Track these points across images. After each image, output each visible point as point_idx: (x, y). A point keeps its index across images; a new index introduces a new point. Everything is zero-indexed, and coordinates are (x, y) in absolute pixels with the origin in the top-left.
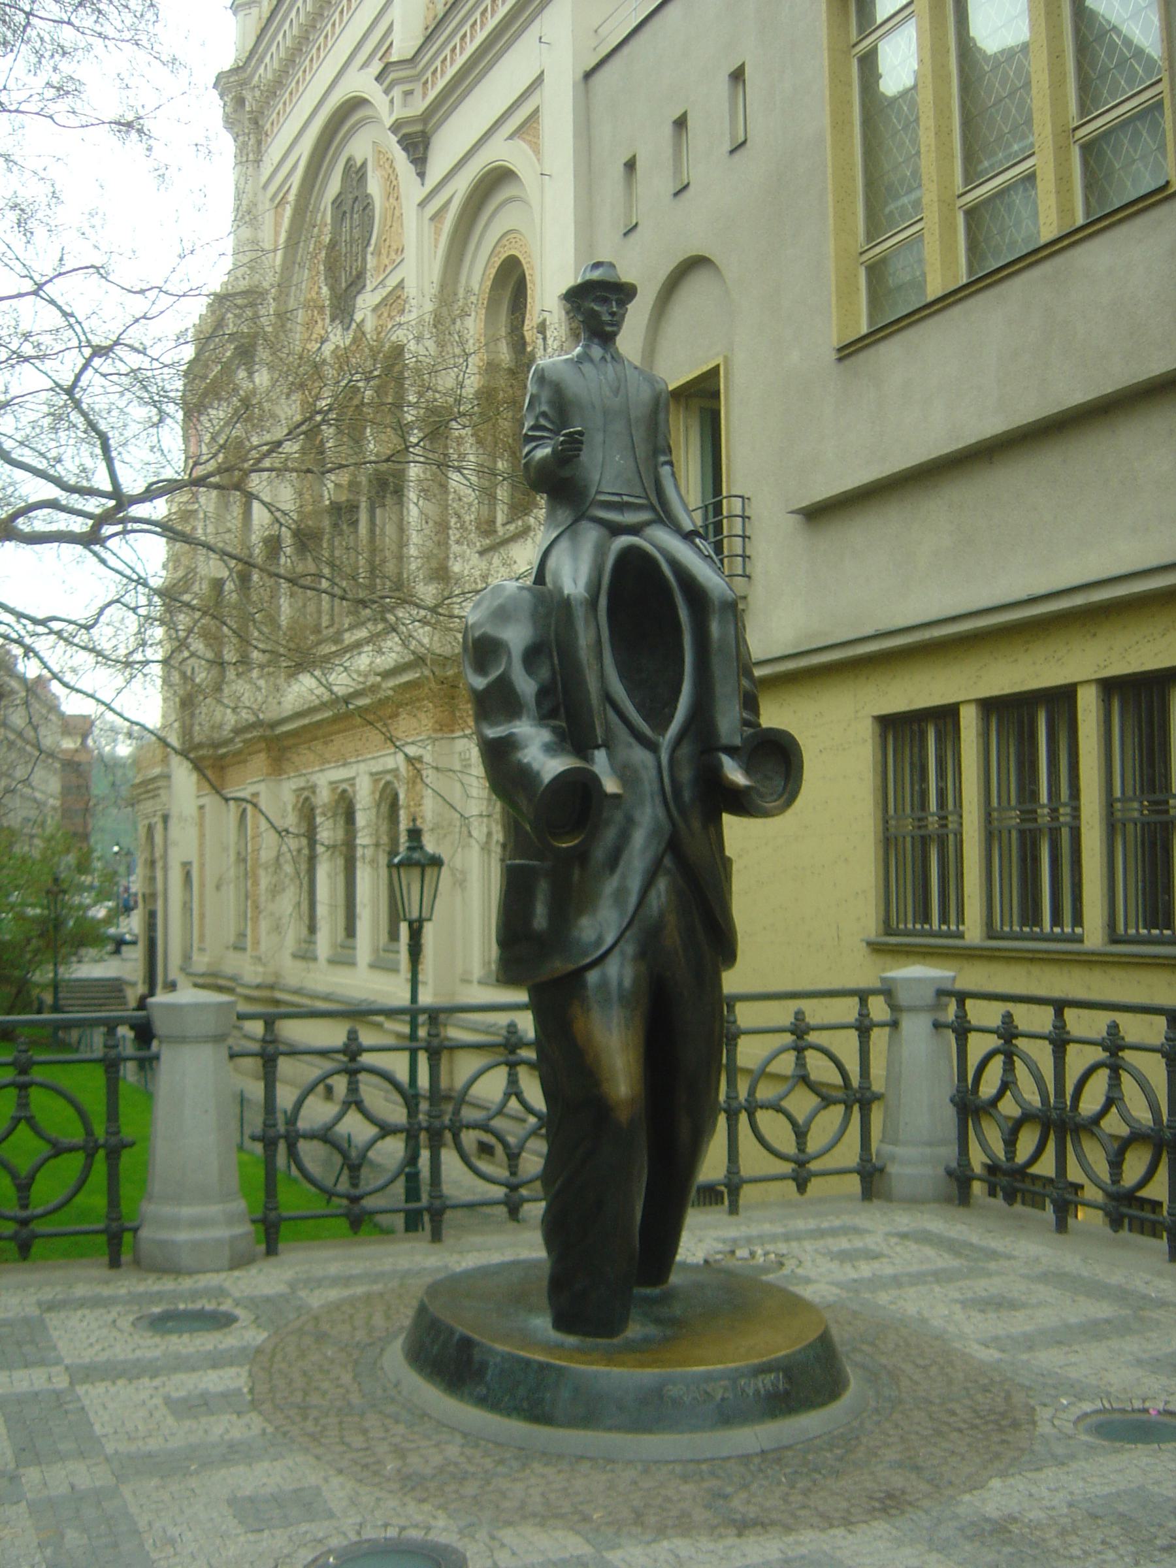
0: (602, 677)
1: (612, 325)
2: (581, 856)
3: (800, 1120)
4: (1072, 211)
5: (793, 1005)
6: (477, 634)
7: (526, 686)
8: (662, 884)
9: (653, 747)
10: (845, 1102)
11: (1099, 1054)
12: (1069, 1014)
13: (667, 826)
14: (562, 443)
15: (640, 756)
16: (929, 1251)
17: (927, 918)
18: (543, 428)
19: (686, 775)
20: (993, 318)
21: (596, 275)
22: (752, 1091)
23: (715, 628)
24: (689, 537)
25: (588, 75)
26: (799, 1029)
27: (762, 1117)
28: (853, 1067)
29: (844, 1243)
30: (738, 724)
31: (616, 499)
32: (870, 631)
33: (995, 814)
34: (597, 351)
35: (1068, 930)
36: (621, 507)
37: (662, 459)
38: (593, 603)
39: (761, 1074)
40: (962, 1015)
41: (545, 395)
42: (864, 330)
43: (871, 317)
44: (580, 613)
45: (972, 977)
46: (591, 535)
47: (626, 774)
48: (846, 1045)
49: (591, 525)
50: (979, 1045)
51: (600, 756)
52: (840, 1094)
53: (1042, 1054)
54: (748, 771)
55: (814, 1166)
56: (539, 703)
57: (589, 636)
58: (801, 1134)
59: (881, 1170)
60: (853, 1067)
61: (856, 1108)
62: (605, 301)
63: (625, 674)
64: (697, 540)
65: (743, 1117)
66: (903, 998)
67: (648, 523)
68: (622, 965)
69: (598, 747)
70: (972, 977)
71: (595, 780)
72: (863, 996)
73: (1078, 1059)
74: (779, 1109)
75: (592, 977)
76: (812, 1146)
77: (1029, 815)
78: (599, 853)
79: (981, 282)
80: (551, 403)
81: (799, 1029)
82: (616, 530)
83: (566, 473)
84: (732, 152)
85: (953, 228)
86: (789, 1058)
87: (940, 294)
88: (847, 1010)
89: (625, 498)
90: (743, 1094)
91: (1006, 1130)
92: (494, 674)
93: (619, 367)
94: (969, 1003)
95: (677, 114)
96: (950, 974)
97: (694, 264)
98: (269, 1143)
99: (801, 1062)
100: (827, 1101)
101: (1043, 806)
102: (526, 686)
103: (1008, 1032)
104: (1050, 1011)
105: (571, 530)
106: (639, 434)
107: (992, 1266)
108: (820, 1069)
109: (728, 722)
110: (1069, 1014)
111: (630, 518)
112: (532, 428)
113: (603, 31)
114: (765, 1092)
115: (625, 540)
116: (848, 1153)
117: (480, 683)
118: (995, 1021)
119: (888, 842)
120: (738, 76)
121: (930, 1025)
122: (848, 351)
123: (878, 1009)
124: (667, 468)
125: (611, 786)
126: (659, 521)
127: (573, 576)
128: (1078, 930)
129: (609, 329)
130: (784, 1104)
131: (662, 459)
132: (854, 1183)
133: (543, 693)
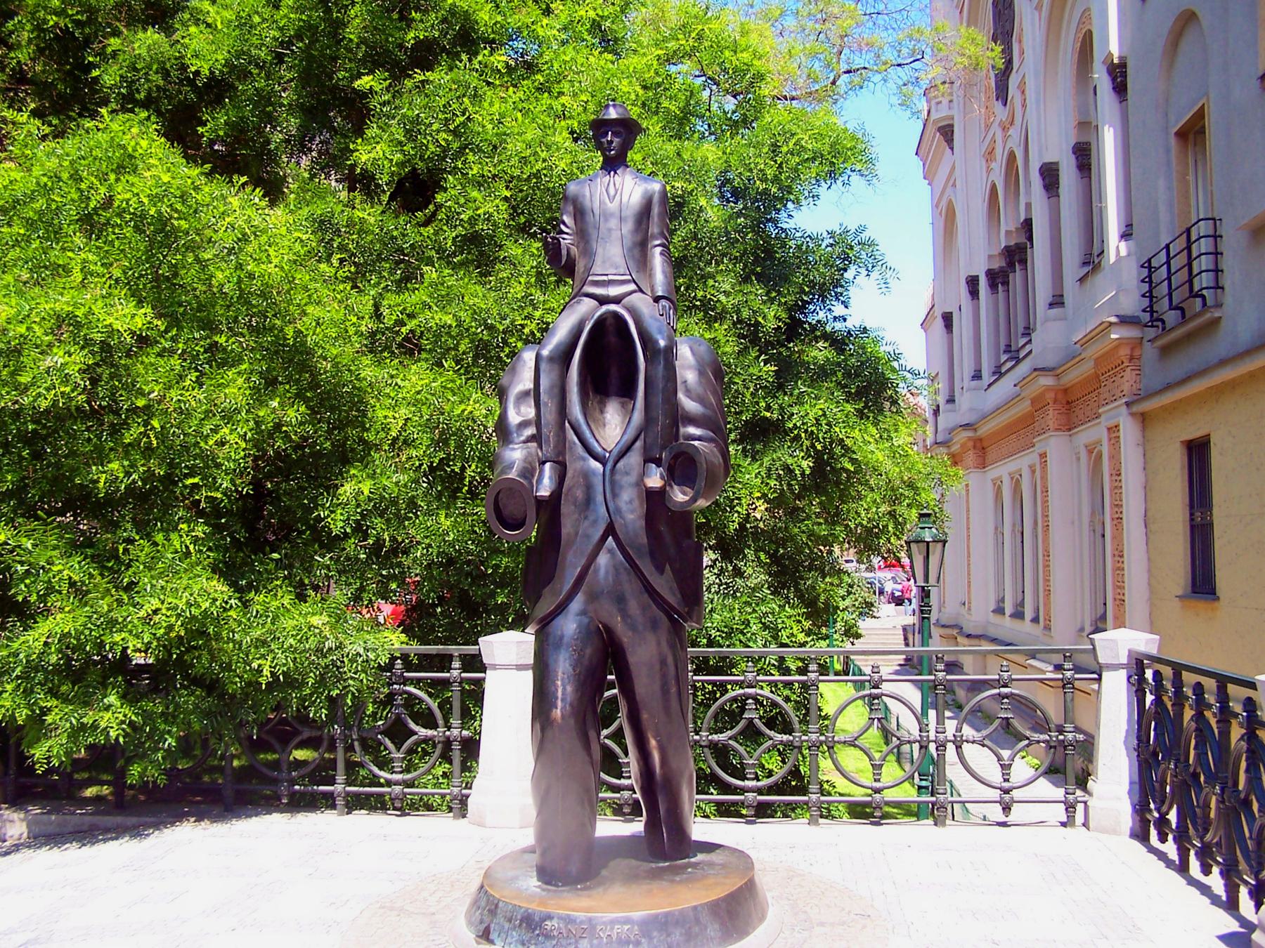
31: (605, 278)
46: (587, 304)
49: (586, 300)
55: (1015, 793)
58: (1006, 768)
65: (951, 748)
89: (611, 277)
106: (628, 227)
111: (613, 291)
115: (605, 308)
126: (641, 291)
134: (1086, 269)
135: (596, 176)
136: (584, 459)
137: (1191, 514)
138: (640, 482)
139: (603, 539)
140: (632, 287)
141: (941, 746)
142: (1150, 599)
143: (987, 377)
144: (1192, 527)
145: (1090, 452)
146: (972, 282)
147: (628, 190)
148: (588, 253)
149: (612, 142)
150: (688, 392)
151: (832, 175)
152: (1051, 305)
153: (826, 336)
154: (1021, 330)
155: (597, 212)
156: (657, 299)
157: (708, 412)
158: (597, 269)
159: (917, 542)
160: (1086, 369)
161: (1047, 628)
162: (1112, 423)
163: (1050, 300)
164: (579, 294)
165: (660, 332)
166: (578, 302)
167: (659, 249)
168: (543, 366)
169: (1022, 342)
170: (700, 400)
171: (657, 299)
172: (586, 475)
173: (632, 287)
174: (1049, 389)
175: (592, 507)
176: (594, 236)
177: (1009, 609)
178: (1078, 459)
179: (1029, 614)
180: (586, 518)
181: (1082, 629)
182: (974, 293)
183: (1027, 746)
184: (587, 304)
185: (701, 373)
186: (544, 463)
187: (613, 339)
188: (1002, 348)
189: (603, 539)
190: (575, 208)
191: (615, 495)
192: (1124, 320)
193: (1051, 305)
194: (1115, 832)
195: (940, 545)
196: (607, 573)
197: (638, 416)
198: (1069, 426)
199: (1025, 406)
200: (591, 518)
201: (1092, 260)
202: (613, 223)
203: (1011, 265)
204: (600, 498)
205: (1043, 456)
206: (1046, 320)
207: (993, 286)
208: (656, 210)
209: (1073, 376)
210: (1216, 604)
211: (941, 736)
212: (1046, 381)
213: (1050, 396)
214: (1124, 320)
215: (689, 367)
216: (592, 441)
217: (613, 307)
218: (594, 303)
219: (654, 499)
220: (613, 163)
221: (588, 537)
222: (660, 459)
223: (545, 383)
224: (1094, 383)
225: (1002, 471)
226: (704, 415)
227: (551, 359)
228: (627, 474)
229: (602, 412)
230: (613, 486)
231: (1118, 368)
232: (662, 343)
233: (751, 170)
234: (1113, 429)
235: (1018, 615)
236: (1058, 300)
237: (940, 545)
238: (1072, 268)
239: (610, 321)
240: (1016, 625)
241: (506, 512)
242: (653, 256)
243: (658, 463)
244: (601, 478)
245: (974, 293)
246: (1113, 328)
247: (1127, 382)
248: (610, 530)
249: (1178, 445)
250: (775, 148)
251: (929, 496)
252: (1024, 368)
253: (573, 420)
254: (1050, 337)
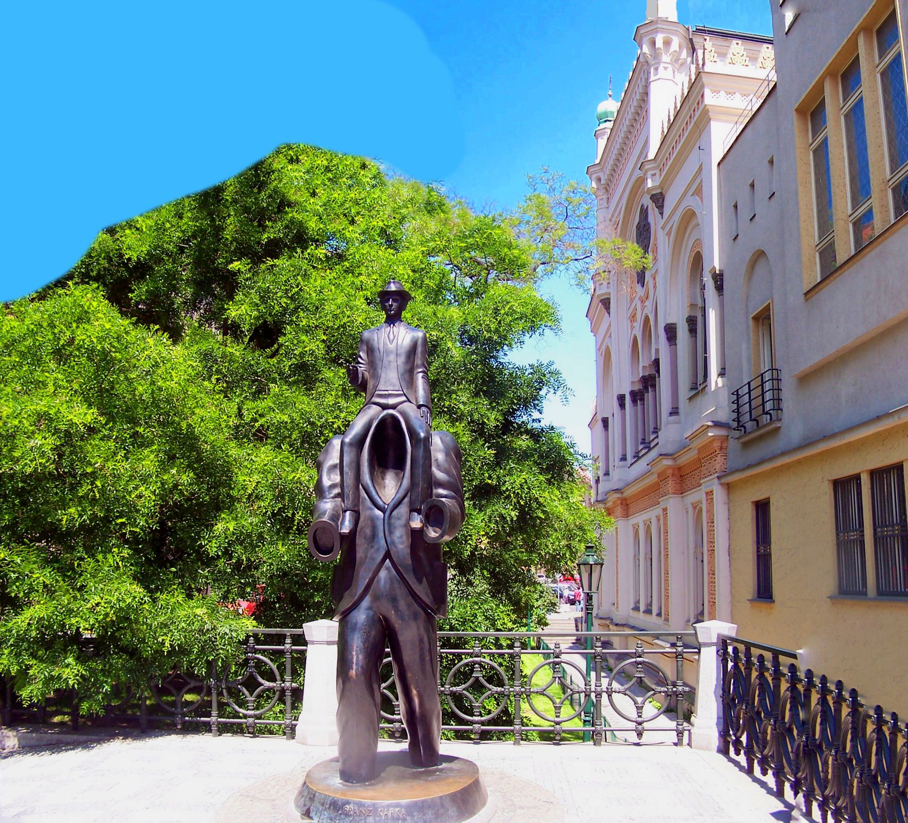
36: (390, 396)
46: (375, 409)
49: (374, 406)
55: (645, 725)
58: (639, 709)
65: (605, 695)
111: (391, 401)
115: (386, 412)
134: (693, 392)
135: (381, 327)
136: (371, 509)
137: (758, 548)
138: (407, 524)
139: (383, 561)
140: (404, 398)
141: (599, 695)
142: (731, 601)
143: (630, 459)
144: (758, 556)
145: (695, 508)
146: (621, 398)
147: (402, 336)
148: (376, 376)
149: (392, 305)
150: (439, 467)
151: (533, 329)
152: (671, 414)
153: (527, 432)
154: (651, 429)
155: (382, 350)
156: (419, 407)
157: (452, 480)
158: (381, 387)
159: (584, 564)
160: (692, 455)
161: (667, 620)
162: (708, 489)
163: (670, 410)
164: (369, 403)
165: (421, 428)
166: (369, 408)
167: (421, 375)
168: (346, 449)
169: (652, 438)
170: (447, 472)
171: (419, 407)
172: (373, 519)
173: (404, 398)
174: (669, 467)
175: (376, 540)
176: (380, 366)
177: (642, 608)
178: (687, 512)
179: (655, 610)
180: (372, 547)
181: (688, 621)
182: (622, 405)
183: (653, 695)
184: (375, 409)
185: (447, 454)
186: (345, 511)
187: (390, 432)
188: (640, 441)
189: (383, 561)
190: (368, 347)
191: (391, 533)
192: (717, 424)
193: (671, 414)
194: (708, 749)
195: (599, 566)
196: (385, 582)
197: (406, 482)
198: (681, 491)
199: (654, 478)
200: (376, 547)
201: (699, 386)
202: (392, 357)
203: (646, 388)
204: (381, 534)
205: (665, 510)
206: (668, 423)
207: (634, 401)
209: (686, 459)
210: (773, 605)
211: (599, 689)
212: (667, 462)
213: (669, 472)
214: (717, 424)
215: (440, 451)
216: (376, 497)
217: (391, 411)
218: (379, 408)
219: (416, 536)
220: (393, 319)
221: (373, 559)
222: (420, 509)
223: (346, 459)
224: (698, 464)
225: (639, 519)
226: (449, 482)
227: (351, 444)
228: (399, 519)
229: (383, 479)
230: (389, 526)
231: (712, 455)
232: (422, 435)
233: (481, 325)
234: (709, 494)
235: (648, 611)
236: (675, 410)
237: (599, 566)
238: (684, 391)
239: (389, 420)
240: (647, 617)
241: (321, 543)
242: (417, 379)
243: (419, 512)
244: (382, 521)
245: (622, 405)
246: (709, 429)
247: (718, 463)
248: (388, 555)
249: (750, 504)
250: (496, 311)
251: (592, 535)
252: (653, 454)
253: (364, 484)
254: (670, 434)
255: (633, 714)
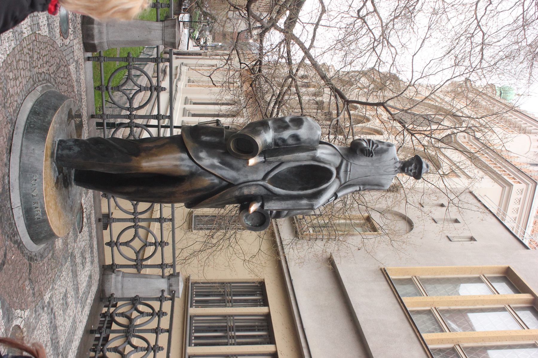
0: (289, 161)
1: (407, 170)
2: (227, 152)
3: (132, 244)
4: (432, 344)
5: (170, 241)
6: (304, 120)
7: (286, 135)
8: (216, 181)
9: (264, 179)
10: (137, 259)
11: (157, 309)
12: (167, 334)
13: (236, 183)
14: (369, 150)
15: (261, 175)
16: (85, 284)
17: (197, 295)
18: (373, 146)
19: (253, 190)
20: (396, 317)
21: (424, 166)
22: (142, 227)
23: (304, 202)
24: (335, 195)
25: (471, 193)
26: (162, 244)
27: (133, 230)
28: (149, 262)
29: (88, 255)
30: (271, 208)
31: (349, 170)
32: (292, 278)
33: (232, 318)
34: (398, 165)
35: (193, 341)
36: (346, 171)
37: (362, 187)
38: (314, 159)
39: (148, 231)
40: (166, 299)
41: (385, 147)
42: (390, 277)
43: (395, 280)
44: (311, 153)
45: (178, 302)
46: (337, 161)
47: (256, 167)
48: (156, 260)
49: (340, 161)
50: (156, 305)
51: (262, 159)
52: (140, 257)
53: (153, 325)
54: (255, 212)
55: (115, 248)
56: (280, 139)
57: (302, 158)
58: (127, 244)
59: (113, 272)
60: (149, 262)
61: (135, 263)
62: (416, 168)
63: (291, 171)
64: (334, 198)
65: (133, 224)
66: (173, 280)
67: (340, 181)
68: (188, 166)
69: (265, 158)
70: (178, 302)
71: (253, 156)
72: (173, 266)
73: (151, 338)
74: (135, 237)
75: (185, 156)
76: (122, 248)
77: (232, 329)
78: (228, 159)
79: (408, 315)
80: (382, 148)
81: (162, 244)
82: (338, 169)
83: (358, 152)
84: (447, 237)
85: (426, 306)
86: (153, 241)
87: (404, 301)
88: (168, 260)
90: (140, 224)
91: (126, 314)
92: (290, 124)
93: (393, 173)
94: (171, 301)
95: (459, 220)
96: (180, 296)
97: (410, 224)
98: (127, 59)
99: (151, 244)
100: (137, 253)
101: (234, 333)
102: (286, 135)
103: (160, 314)
104: (167, 327)
105: (337, 153)
107: (79, 305)
108: (150, 250)
109: (272, 206)
110: (167, 334)
112: (373, 142)
113: (485, 198)
114: (141, 232)
116: (119, 260)
117: (287, 120)
118: (164, 310)
119: (223, 284)
120: (472, 239)
121: (163, 289)
122: (384, 272)
123: (168, 271)
124: (358, 189)
125: (252, 161)
126: (341, 185)
127: (323, 153)
128: (193, 345)
129: (406, 169)
130: (137, 239)
131: (362, 187)
132: (108, 262)
133: (284, 140)
140: (343, 182)
208: (376, 187)
255: (123, 239)
